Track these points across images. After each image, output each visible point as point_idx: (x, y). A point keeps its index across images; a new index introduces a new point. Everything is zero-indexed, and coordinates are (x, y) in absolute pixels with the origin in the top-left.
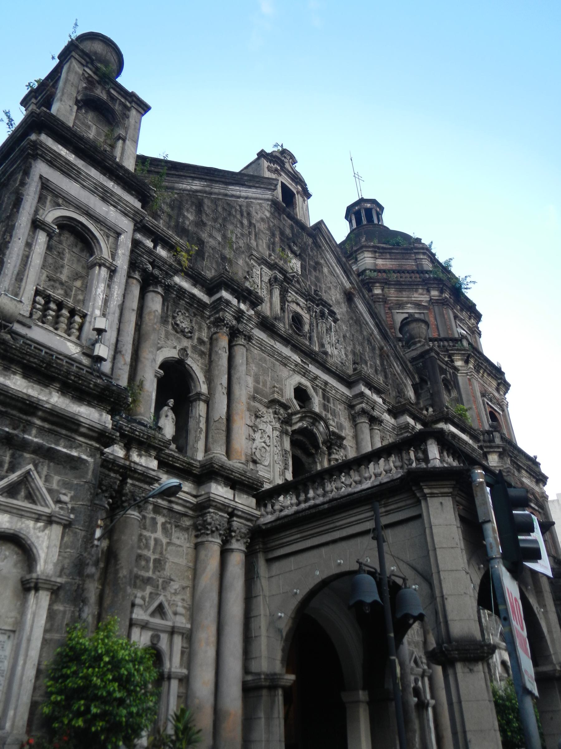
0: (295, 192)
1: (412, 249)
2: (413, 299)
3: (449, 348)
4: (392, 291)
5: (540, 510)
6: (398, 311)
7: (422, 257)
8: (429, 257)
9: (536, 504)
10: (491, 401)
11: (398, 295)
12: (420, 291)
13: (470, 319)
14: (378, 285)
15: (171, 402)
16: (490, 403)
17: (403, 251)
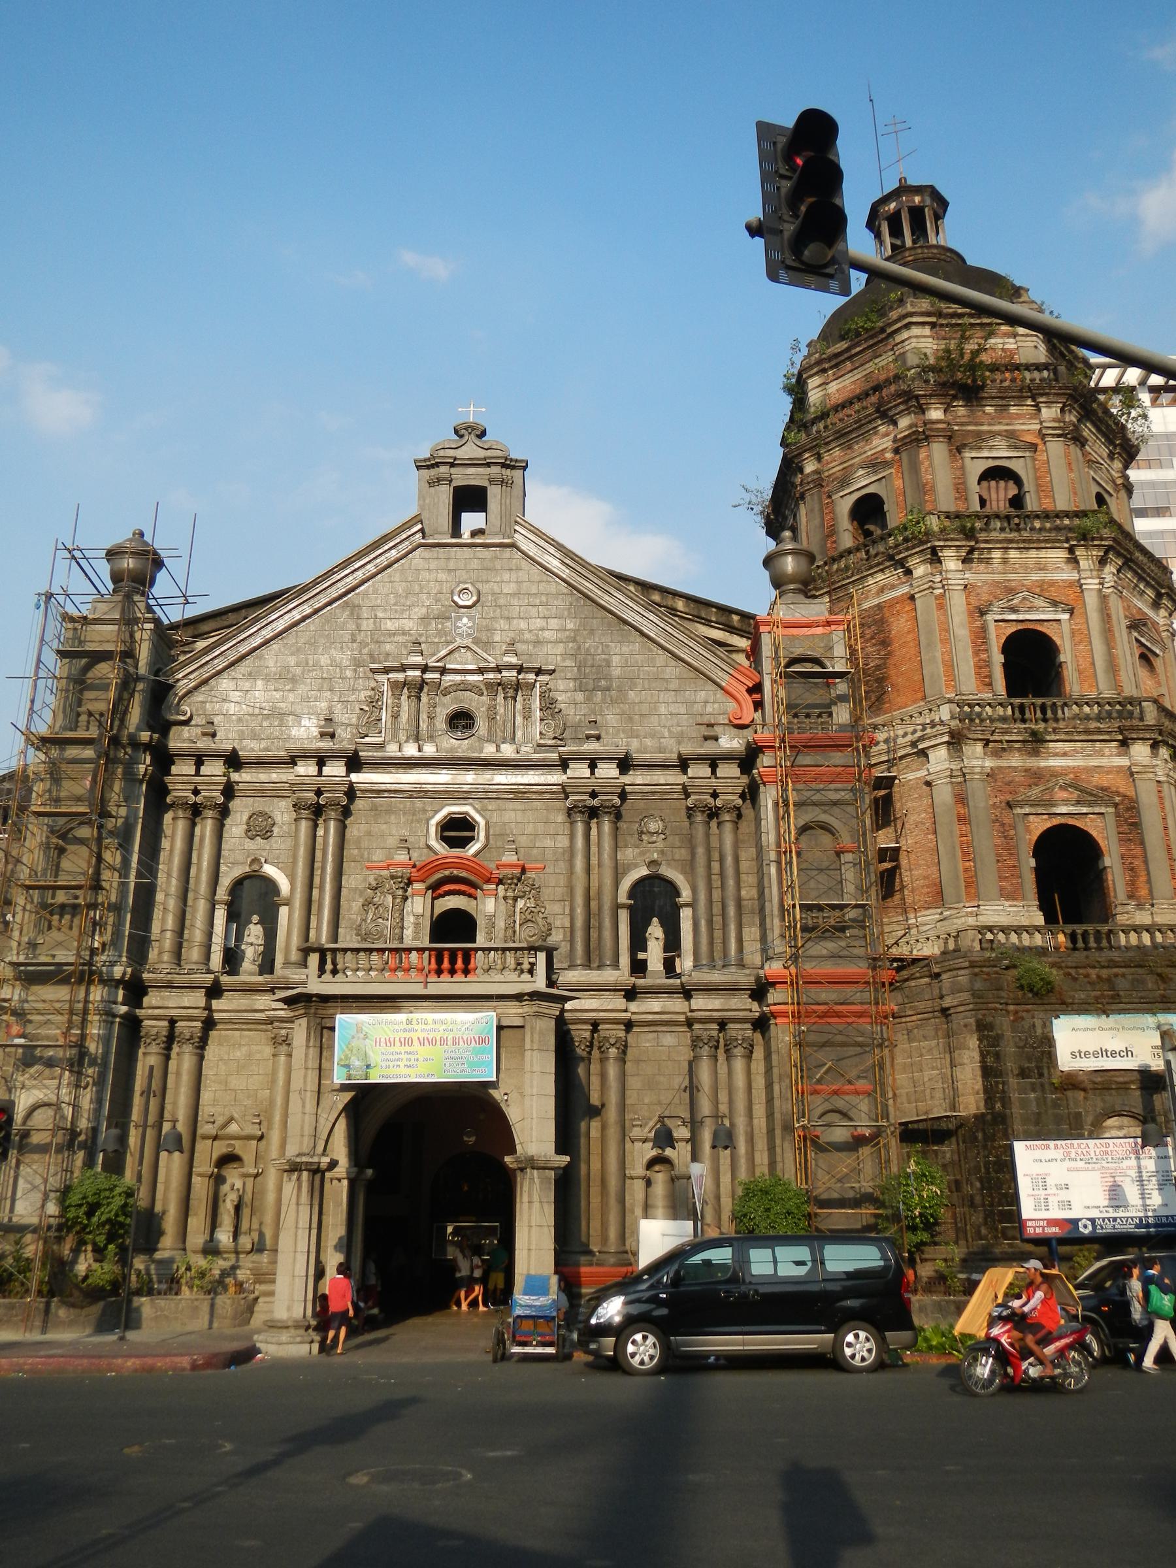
0: (485, 483)
1: (883, 330)
2: (869, 453)
3: (891, 552)
4: (837, 452)
5: (1097, 810)
6: (842, 494)
7: (905, 335)
8: (923, 324)
9: (1078, 802)
10: (1014, 610)
11: (847, 457)
12: (882, 429)
13: (1039, 410)
14: (807, 455)
15: (255, 918)
16: (1013, 617)
17: (871, 342)
